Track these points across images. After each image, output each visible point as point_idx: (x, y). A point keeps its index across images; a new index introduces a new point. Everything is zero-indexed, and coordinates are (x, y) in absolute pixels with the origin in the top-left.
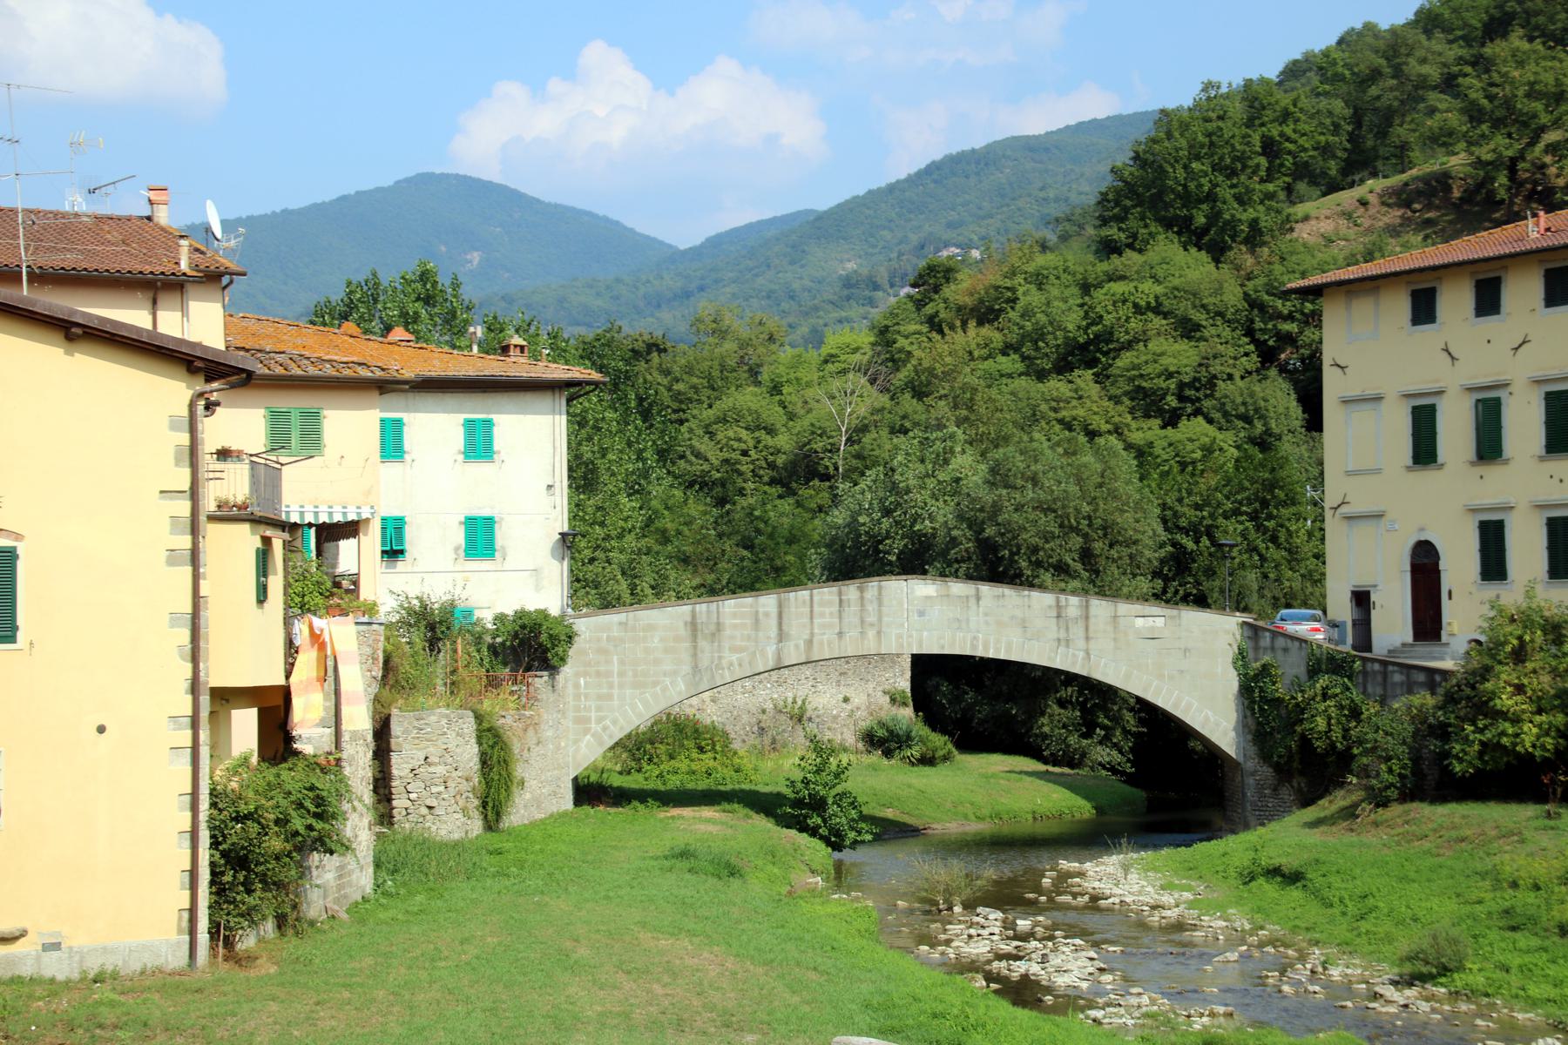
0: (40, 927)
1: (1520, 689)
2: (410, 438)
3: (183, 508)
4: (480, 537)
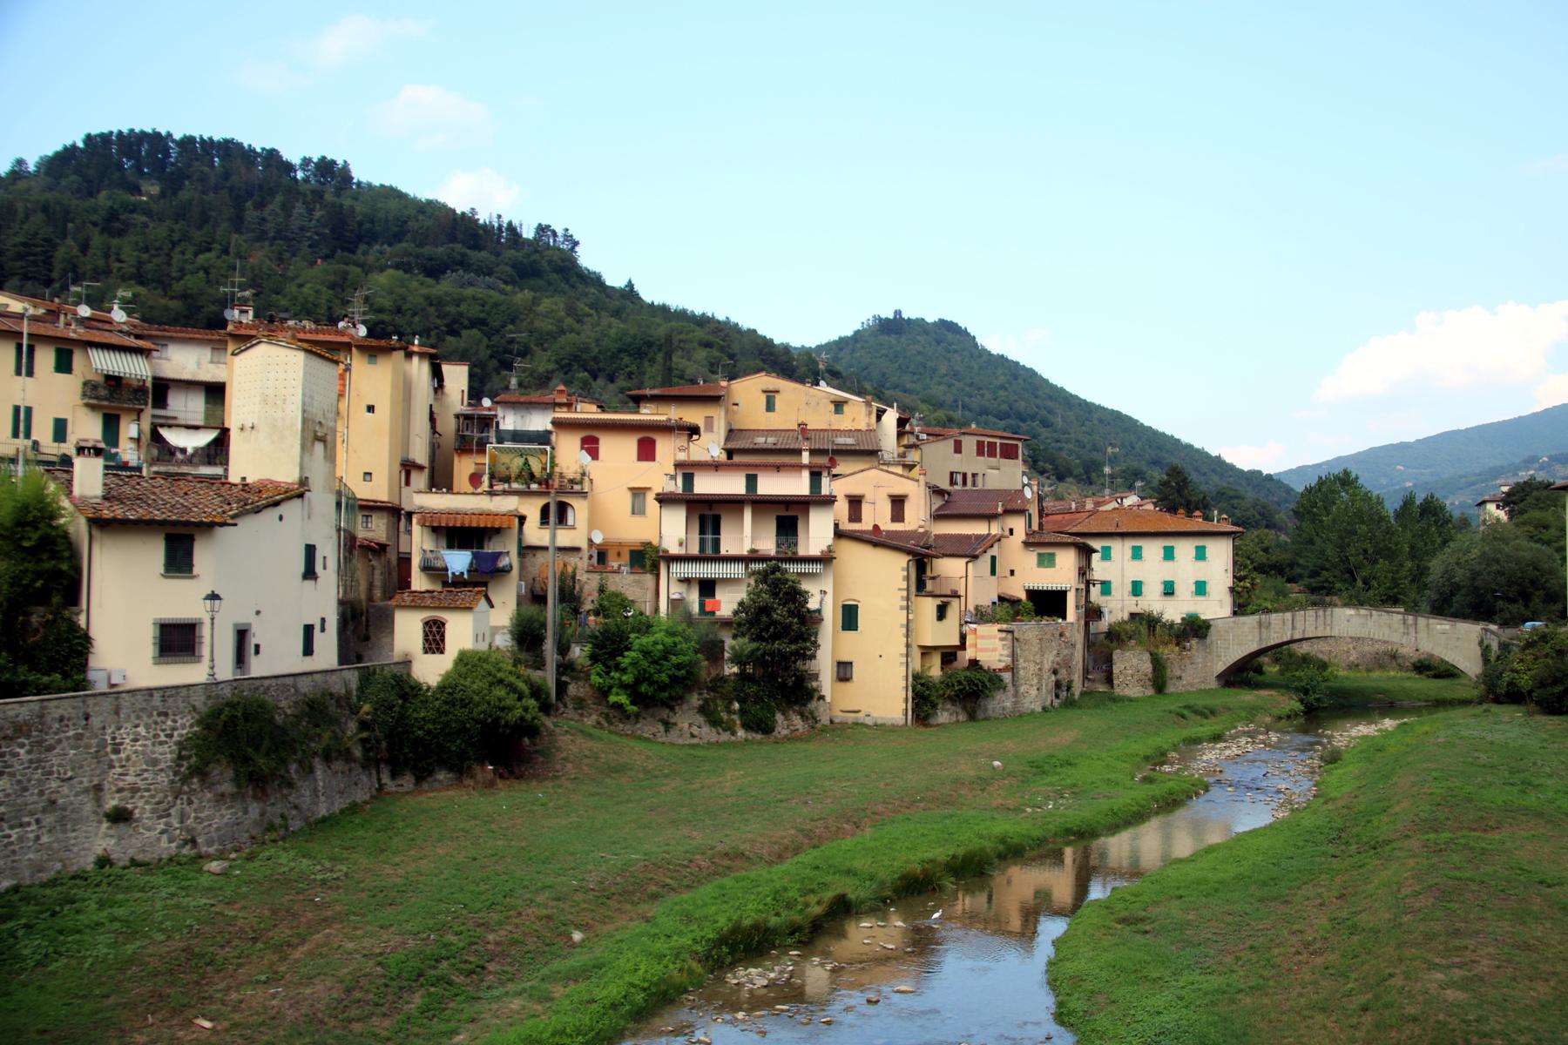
0: (865, 709)
1: (1522, 661)
2: (1176, 553)
3: (905, 593)
4: (1201, 588)
